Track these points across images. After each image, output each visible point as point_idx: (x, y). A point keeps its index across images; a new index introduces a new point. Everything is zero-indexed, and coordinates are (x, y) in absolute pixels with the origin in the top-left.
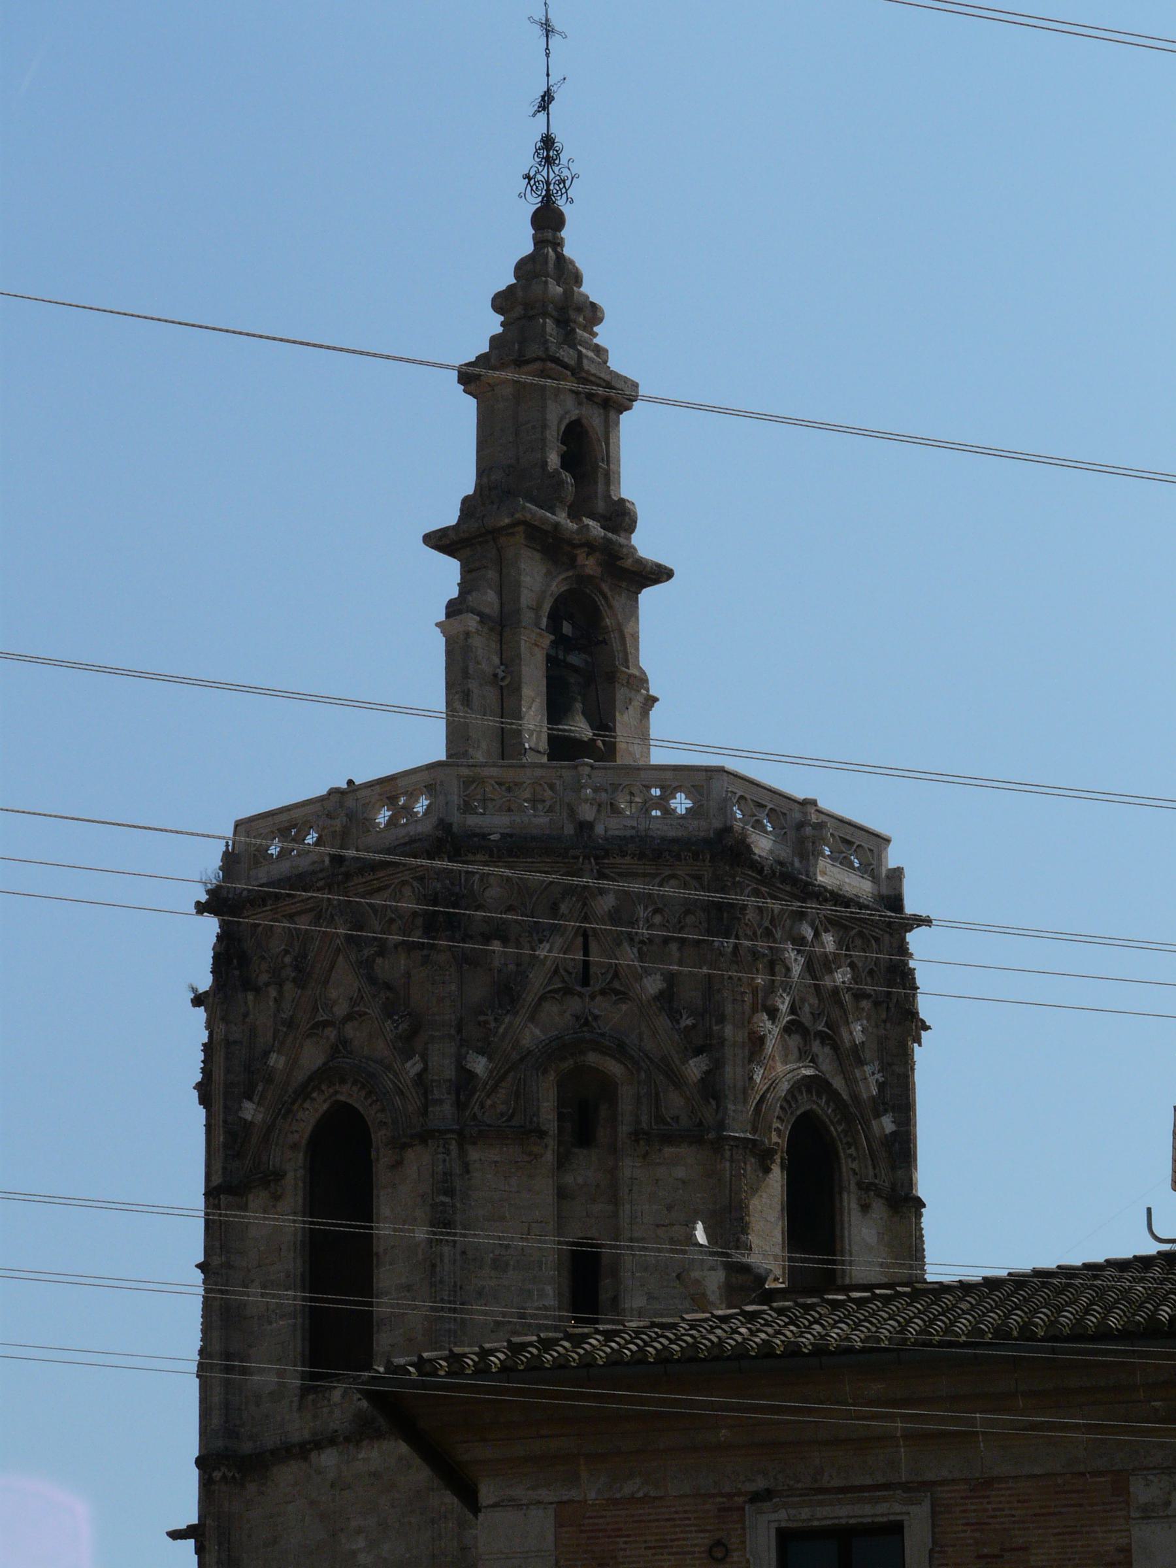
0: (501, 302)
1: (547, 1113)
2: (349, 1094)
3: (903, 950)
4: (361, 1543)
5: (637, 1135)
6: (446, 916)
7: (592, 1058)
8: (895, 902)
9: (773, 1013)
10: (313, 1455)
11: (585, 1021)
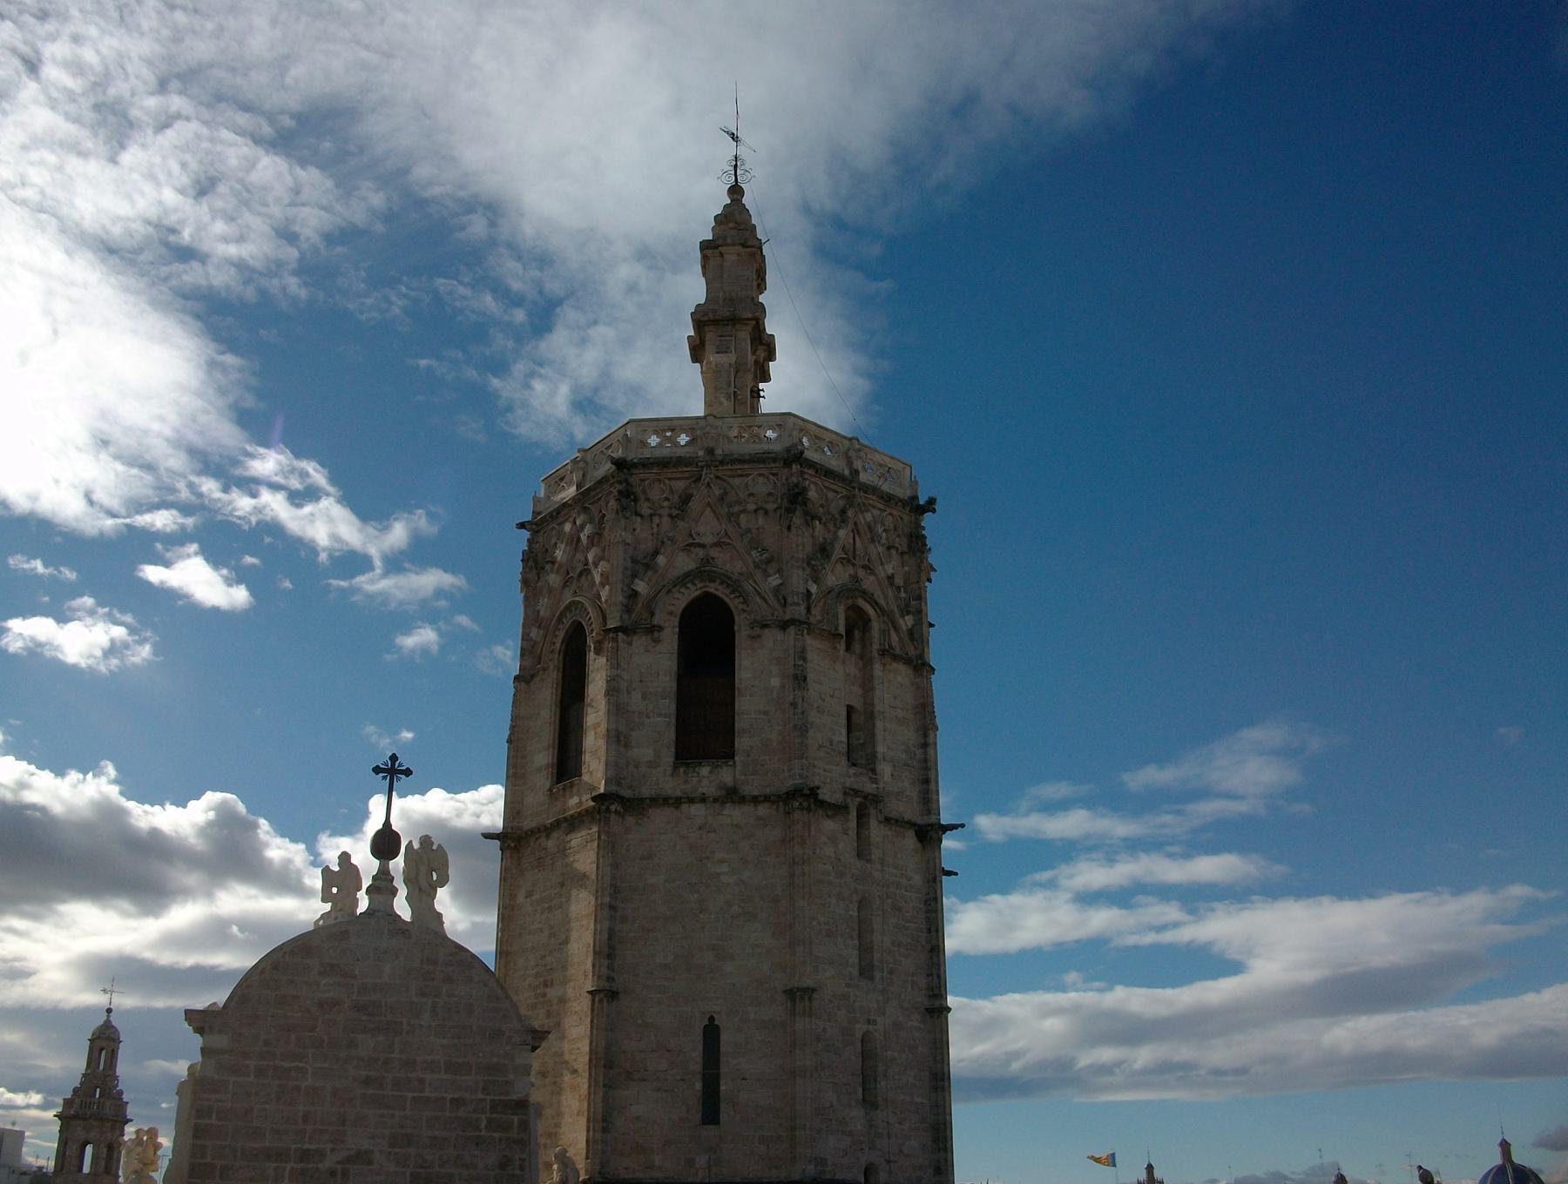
4: (724, 868)
10: (684, 807)
11: (856, 579)
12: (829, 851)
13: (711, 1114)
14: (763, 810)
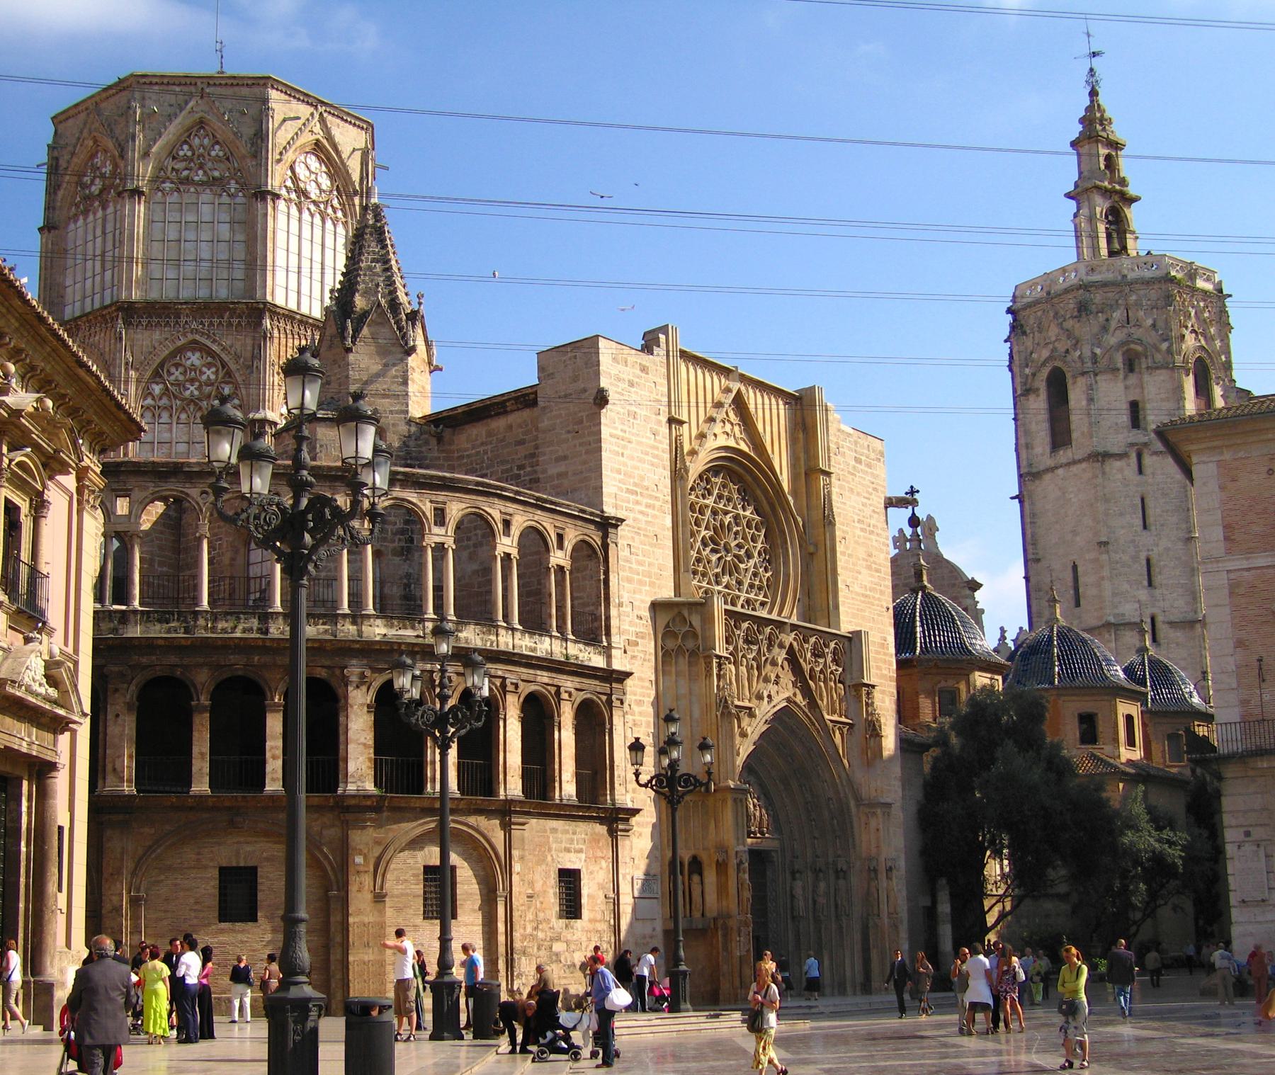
0: (1082, 121)
1: (1120, 365)
2: (1058, 364)
3: (1225, 306)
5: (1148, 368)
6: (1083, 309)
7: (1132, 346)
8: (1221, 291)
9: (1187, 327)
12: (1119, 476)
13: (1078, 604)
14: (1084, 465)
